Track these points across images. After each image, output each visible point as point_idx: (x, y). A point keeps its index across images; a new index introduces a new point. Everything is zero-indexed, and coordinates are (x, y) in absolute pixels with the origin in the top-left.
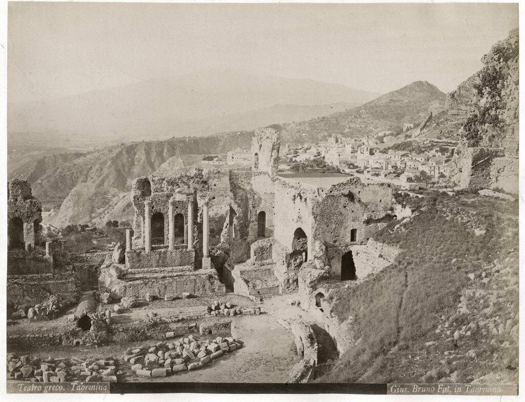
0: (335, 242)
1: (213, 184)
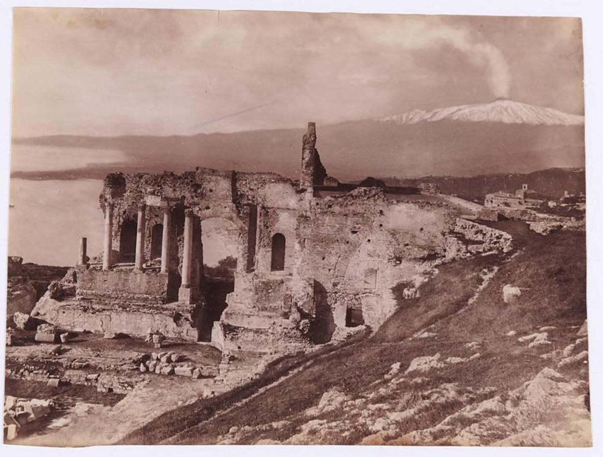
0: (335, 285)
1: (209, 189)
